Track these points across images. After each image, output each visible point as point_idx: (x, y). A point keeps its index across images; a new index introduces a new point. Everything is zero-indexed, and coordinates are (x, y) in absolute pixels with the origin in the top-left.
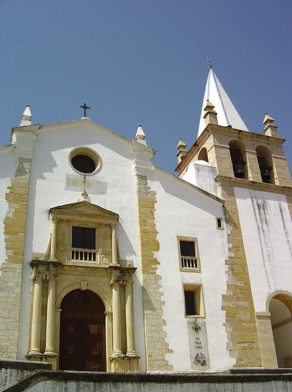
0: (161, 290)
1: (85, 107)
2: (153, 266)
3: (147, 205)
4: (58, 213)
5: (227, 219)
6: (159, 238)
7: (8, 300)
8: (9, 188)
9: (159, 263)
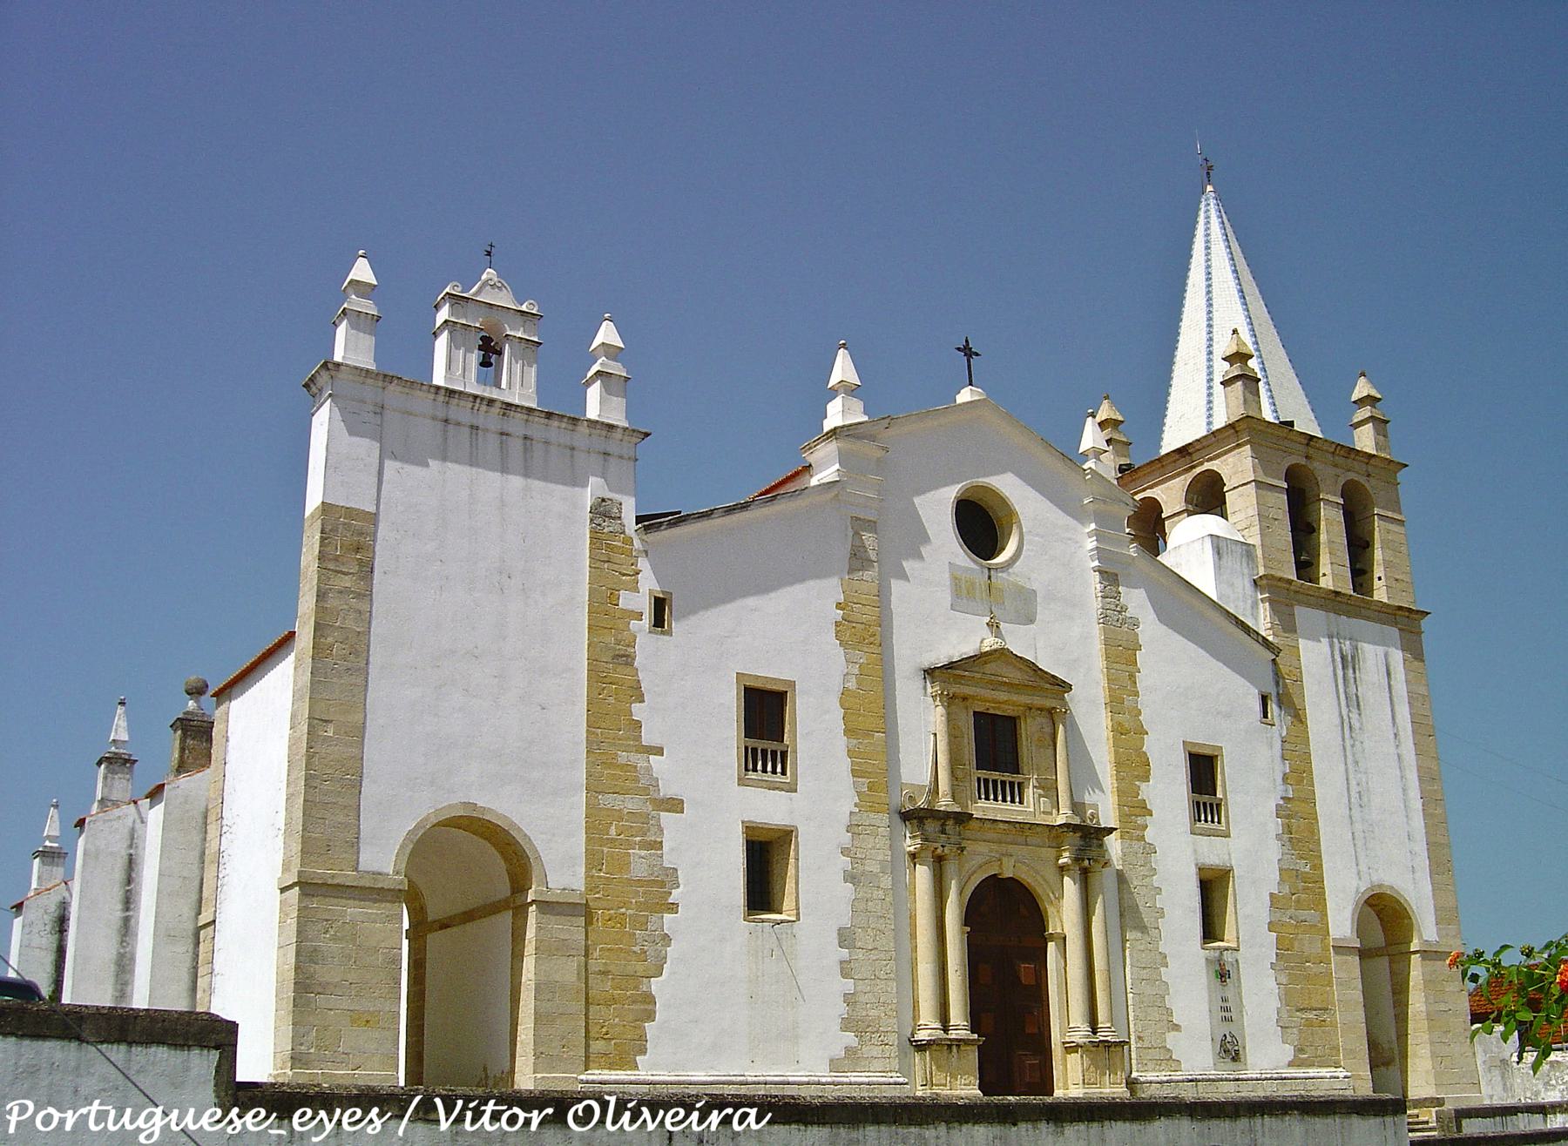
1: (968, 352)
2: (1140, 820)
3: (1122, 652)
4: (947, 676)
5: (1280, 697)
8: (839, 606)
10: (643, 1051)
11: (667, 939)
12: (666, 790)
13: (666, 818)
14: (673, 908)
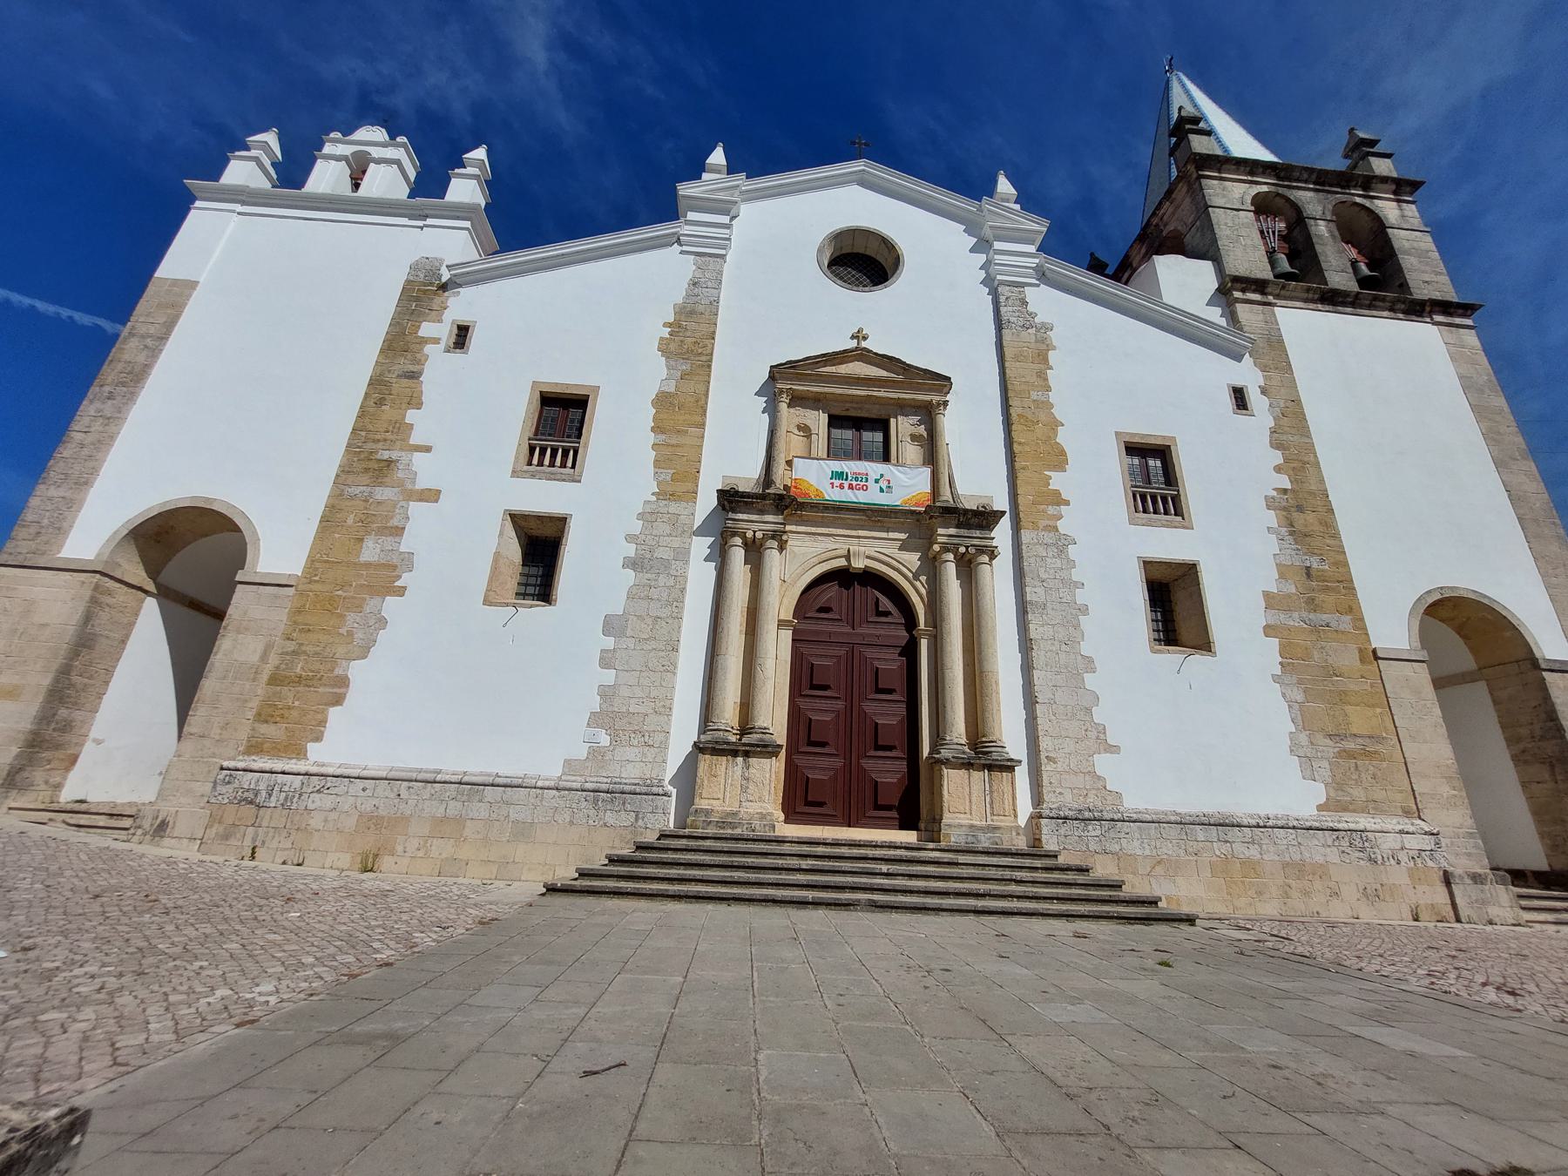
0: (1076, 575)
2: (1051, 510)
4: (789, 383)
6: (1062, 437)
7: (654, 593)
9: (1067, 503)
10: (318, 739)
11: (382, 622)
12: (422, 483)
13: (415, 508)
14: (401, 592)
